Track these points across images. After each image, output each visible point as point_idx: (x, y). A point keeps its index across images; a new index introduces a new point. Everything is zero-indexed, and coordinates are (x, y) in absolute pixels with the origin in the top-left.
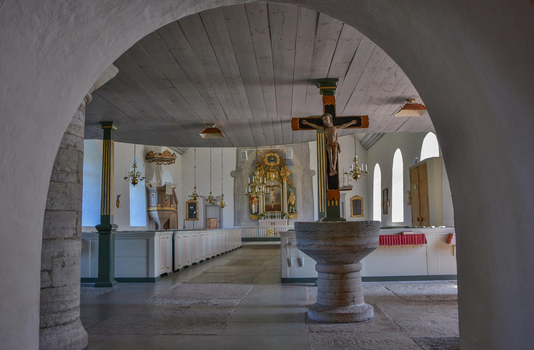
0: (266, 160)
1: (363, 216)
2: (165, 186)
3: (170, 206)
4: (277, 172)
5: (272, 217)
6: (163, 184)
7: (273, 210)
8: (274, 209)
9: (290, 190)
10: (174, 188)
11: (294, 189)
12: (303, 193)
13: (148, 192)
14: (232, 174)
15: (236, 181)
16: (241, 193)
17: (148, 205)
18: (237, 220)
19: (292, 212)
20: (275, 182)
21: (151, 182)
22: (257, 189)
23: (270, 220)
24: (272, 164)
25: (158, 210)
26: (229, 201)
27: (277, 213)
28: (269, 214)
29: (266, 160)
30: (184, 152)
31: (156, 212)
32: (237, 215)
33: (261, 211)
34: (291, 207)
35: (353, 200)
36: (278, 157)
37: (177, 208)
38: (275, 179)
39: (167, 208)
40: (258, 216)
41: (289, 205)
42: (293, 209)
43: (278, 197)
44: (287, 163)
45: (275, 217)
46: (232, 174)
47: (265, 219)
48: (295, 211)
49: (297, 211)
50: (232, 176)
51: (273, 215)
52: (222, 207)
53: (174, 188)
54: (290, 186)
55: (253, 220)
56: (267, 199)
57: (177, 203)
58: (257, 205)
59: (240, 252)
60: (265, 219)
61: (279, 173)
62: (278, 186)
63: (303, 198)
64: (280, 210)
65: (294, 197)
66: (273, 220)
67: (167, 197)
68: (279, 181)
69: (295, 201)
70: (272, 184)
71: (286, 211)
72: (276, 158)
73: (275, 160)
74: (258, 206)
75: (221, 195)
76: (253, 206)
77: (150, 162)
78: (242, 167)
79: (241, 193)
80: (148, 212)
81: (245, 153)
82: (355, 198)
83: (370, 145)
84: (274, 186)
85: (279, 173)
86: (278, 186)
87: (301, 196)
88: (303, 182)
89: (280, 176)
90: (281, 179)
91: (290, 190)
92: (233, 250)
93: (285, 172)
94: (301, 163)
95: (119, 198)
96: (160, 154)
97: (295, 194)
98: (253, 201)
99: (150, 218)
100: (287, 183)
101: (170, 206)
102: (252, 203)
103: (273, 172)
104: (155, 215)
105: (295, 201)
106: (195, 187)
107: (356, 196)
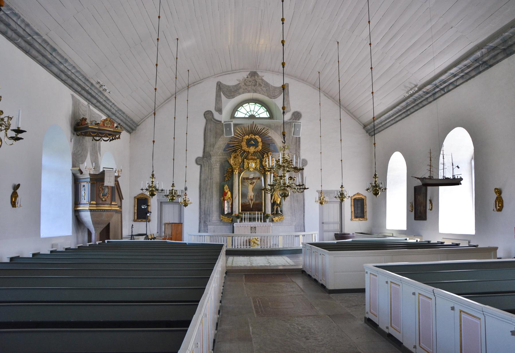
0: (244, 144)
1: (367, 219)
2: (103, 173)
3: (111, 204)
4: (258, 161)
5: (250, 220)
6: (101, 170)
7: (251, 210)
8: (253, 209)
10: (118, 177)
13: (76, 182)
14: (198, 161)
15: (203, 169)
16: (209, 187)
17: (76, 202)
20: (255, 173)
21: (83, 167)
23: (248, 224)
24: (252, 149)
25: (91, 210)
27: (257, 214)
28: (247, 215)
29: (244, 144)
30: (133, 130)
31: (89, 213)
32: (203, 216)
34: (275, 207)
35: (354, 199)
36: (260, 140)
37: (121, 207)
38: (255, 169)
39: (106, 207)
40: (231, 218)
42: (279, 208)
44: (271, 148)
45: (254, 219)
46: (198, 161)
47: (241, 221)
48: (281, 211)
51: (252, 216)
52: (186, 205)
53: (118, 177)
55: (224, 223)
56: (244, 195)
57: (121, 198)
58: (230, 203)
60: (241, 221)
61: (261, 162)
64: (260, 210)
66: (253, 224)
67: (106, 190)
68: (260, 171)
70: (252, 176)
71: (269, 211)
73: (256, 145)
75: (183, 189)
76: (226, 205)
77: (81, 135)
78: (211, 153)
79: (209, 187)
81: (230, 124)
83: (380, 129)
84: (253, 178)
85: (261, 162)
95: (18, 191)
96: (97, 124)
98: (226, 198)
99: (78, 222)
101: (111, 204)
102: (224, 200)
104: (87, 217)
106: (153, 175)
107: (358, 194)
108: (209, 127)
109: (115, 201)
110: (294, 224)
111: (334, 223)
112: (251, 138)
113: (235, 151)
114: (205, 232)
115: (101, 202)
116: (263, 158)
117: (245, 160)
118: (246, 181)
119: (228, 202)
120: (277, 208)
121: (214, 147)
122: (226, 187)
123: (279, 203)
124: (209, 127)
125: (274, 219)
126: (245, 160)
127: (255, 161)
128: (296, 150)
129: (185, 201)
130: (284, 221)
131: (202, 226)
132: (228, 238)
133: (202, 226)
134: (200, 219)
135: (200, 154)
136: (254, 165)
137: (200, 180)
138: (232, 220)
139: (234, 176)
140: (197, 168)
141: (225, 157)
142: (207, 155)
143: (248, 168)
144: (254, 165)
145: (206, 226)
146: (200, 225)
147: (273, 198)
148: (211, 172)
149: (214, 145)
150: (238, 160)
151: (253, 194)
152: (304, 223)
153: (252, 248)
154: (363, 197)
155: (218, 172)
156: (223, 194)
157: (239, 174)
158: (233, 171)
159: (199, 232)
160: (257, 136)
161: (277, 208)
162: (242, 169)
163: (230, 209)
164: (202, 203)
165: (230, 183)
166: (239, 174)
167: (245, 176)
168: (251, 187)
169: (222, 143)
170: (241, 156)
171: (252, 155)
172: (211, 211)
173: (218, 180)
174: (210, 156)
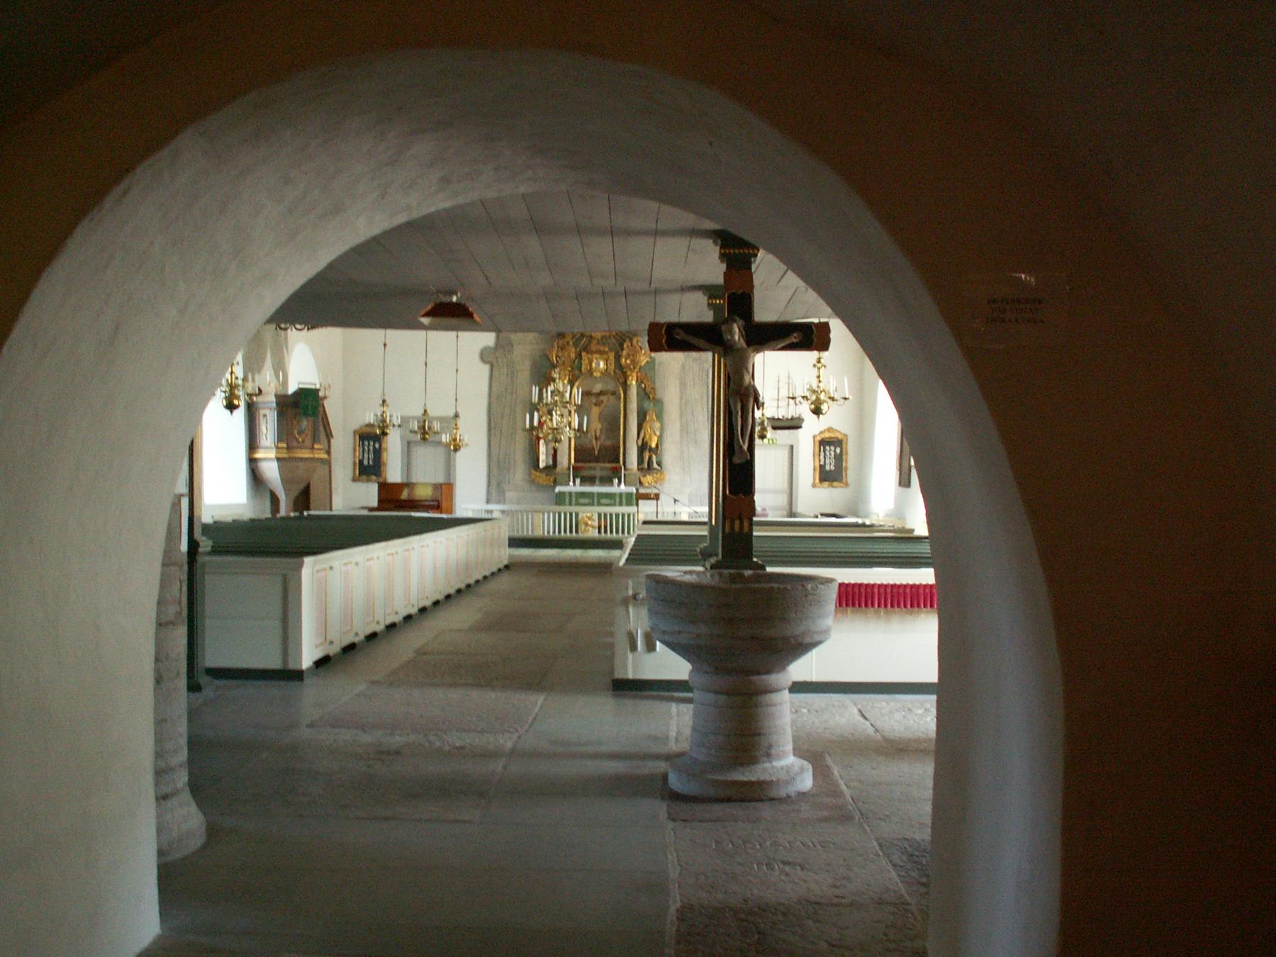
1: (847, 485)
4: (612, 356)
9: (646, 405)
11: (658, 403)
12: (681, 415)
15: (496, 373)
16: (507, 410)
17: (252, 445)
18: (496, 487)
22: (556, 418)
25: (278, 459)
26: (473, 431)
31: (275, 465)
33: (563, 461)
37: (329, 453)
38: (606, 373)
39: (305, 454)
41: (643, 448)
42: (654, 457)
43: (613, 425)
48: (659, 464)
52: (456, 450)
54: (647, 394)
57: (329, 435)
59: (505, 582)
61: (618, 358)
62: (614, 393)
63: (682, 430)
65: (657, 425)
69: (660, 438)
70: (598, 388)
76: (542, 448)
80: (253, 463)
82: (827, 435)
84: (601, 393)
85: (618, 358)
86: (614, 393)
88: (683, 385)
90: (621, 375)
91: (646, 405)
92: (485, 578)
97: (660, 417)
100: (639, 386)
102: (538, 439)
103: (601, 353)
104: (271, 470)
105: (660, 438)
107: (830, 430)
109: (319, 443)
111: (775, 492)
114: (499, 502)
115: (295, 444)
119: (547, 444)
123: (653, 445)
125: (643, 480)
129: (455, 440)
132: (536, 515)
134: (489, 477)
137: (490, 396)
138: (555, 481)
143: (591, 372)
144: (602, 365)
146: (488, 492)
147: (642, 435)
153: (581, 535)
154: (840, 437)
159: (488, 502)
161: (650, 458)
162: (577, 372)
168: (596, 410)
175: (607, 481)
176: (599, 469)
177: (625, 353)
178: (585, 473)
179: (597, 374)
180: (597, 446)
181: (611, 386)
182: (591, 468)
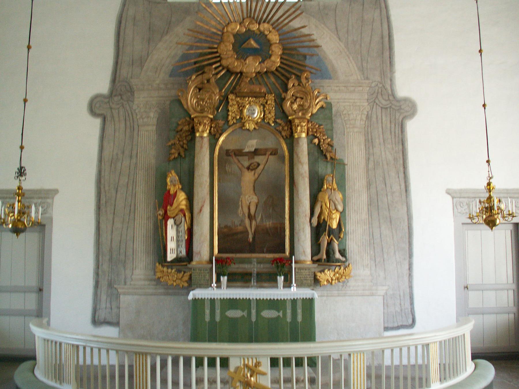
0: (227, 49)
4: (271, 99)
9: (323, 168)
11: (338, 165)
12: (369, 185)
14: (95, 107)
15: (109, 130)
16: (124, 180)
19: (330, 257)
24: (252, 66)
29: (227, 49)
32: (105, 267)
34: (324, 240)
36: (274, 37)
38: (262, 124)
41: (319, 230)
42: (336, 244)
46: (95, 107)
48: (343, 253)
49: (349, 254)
50: (93, 110)
54: (322, 153)
56: (227, 204)
58: (184, 227)
61: (280, 102)
62: (274, 152)
63: (370, 203)
65: (339, 196)
70: (252, 145)
72: (269, 44)
74: (190, 232)
76: (171, 232)
78: (134, 82)
84: (256, 152)
85: (280, 102)
86: (274, 152)
87: (364, 197)
88: (369, 143)
89: (282, 113)
90: (286, 127)
91: (323, 168)
93: (305, 94)
94: (362, 69)
97: (342, 187)
98: (171, 210)
100: (310, 142)
102: (166, 218)
105: (343, 214)
108: (131, 12)
110: (382, 290)
112: (249, 31)
113: (200, 70)
116: (286, 90)
117: (231, 97)
118: (234, 159)
119: (177, 225)
120: (330, 244)
121: (142, 66)
122: (172, 177)
123: (335, 226)
124: (131, 12)
126: (231, 97)
127: (262, 100)
128: (383, 74)
130: (352, 283)
131: (104, 297)
133: (104, 297)
134: (97, 274)
135: (103, 87)
136: (257, 114)
139: (198, 145)
140: (95, 125)
141: (173, 93)
142: (121, 88)
144: (257, 114)
145: (114, 296)
148: (132, 137)
149: (142, 62)
150: (210, 98)
151: (255, 199)
152: (411, 287)
155: (154, 137)
156: (166, 199)
157: (214, 137)
158: (193, 131)
160: (266, 25)
161: (330, 244)
162: (221, 122)
163: (183, 244)
164: (103, 226)
165: (185, 165)
166: (214, 137)
167: (231, 147)
169: (167, 52)
170: (220, 83)
171: (251, 82)
172: (130, 252)
173: (153, 161)
174: (131, 91)
175: (268, 279)
176: (256, 262)
177: (290, 93)
178: (234, 268)
179: (250, 126)
180: (251, 228)
181: (270, 143)
182: (243, 261)
